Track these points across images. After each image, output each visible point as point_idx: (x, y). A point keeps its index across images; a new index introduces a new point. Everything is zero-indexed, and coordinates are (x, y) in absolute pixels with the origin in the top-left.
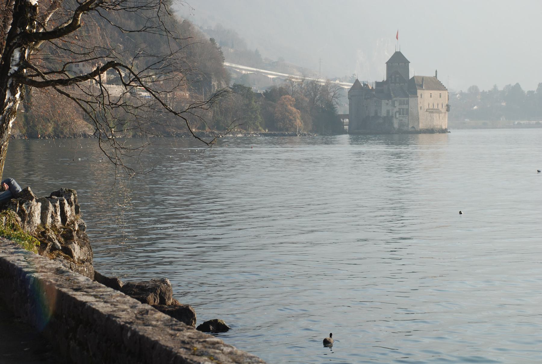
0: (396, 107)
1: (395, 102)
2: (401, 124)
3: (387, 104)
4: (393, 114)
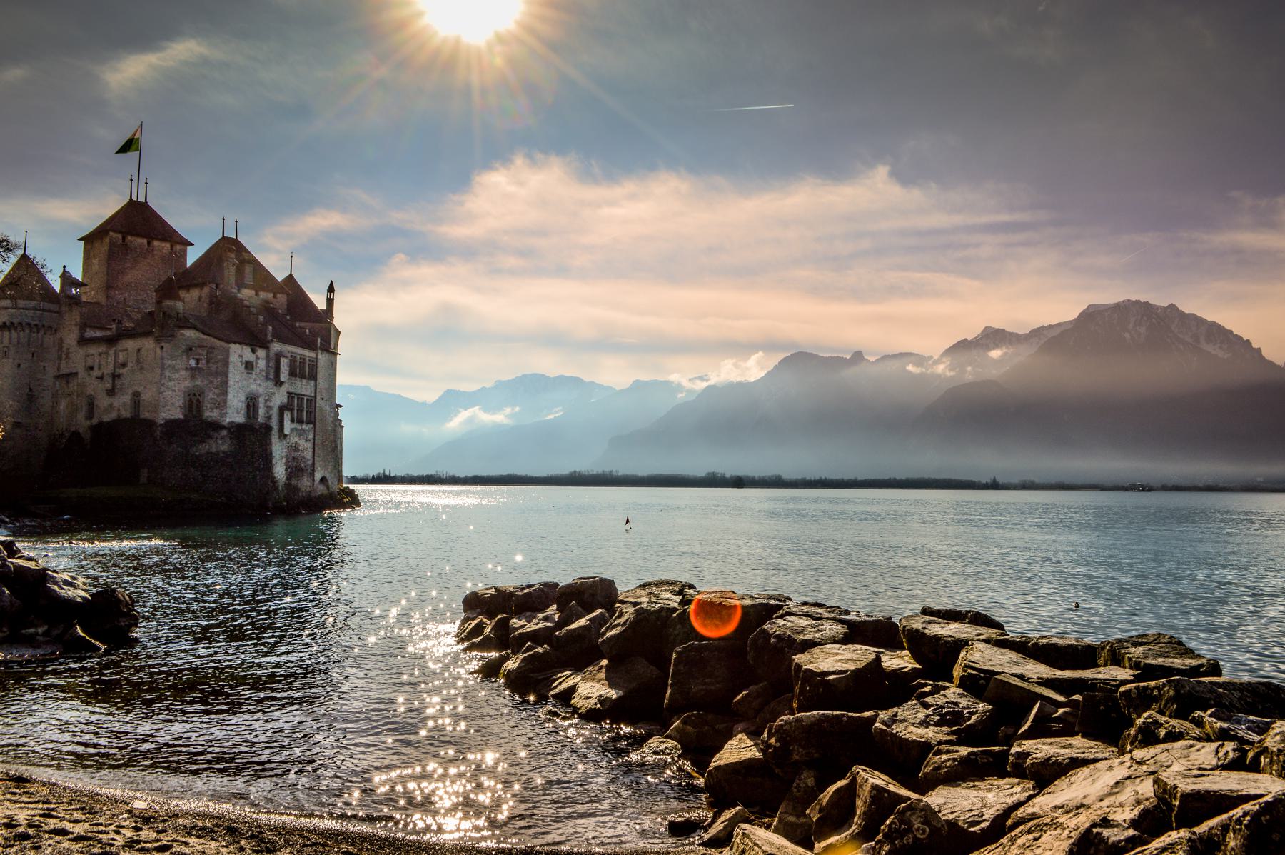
0: (282, 383)
1: (282, 359)
2: (296, 469)
3: (249, 366)
4: (269, 418)
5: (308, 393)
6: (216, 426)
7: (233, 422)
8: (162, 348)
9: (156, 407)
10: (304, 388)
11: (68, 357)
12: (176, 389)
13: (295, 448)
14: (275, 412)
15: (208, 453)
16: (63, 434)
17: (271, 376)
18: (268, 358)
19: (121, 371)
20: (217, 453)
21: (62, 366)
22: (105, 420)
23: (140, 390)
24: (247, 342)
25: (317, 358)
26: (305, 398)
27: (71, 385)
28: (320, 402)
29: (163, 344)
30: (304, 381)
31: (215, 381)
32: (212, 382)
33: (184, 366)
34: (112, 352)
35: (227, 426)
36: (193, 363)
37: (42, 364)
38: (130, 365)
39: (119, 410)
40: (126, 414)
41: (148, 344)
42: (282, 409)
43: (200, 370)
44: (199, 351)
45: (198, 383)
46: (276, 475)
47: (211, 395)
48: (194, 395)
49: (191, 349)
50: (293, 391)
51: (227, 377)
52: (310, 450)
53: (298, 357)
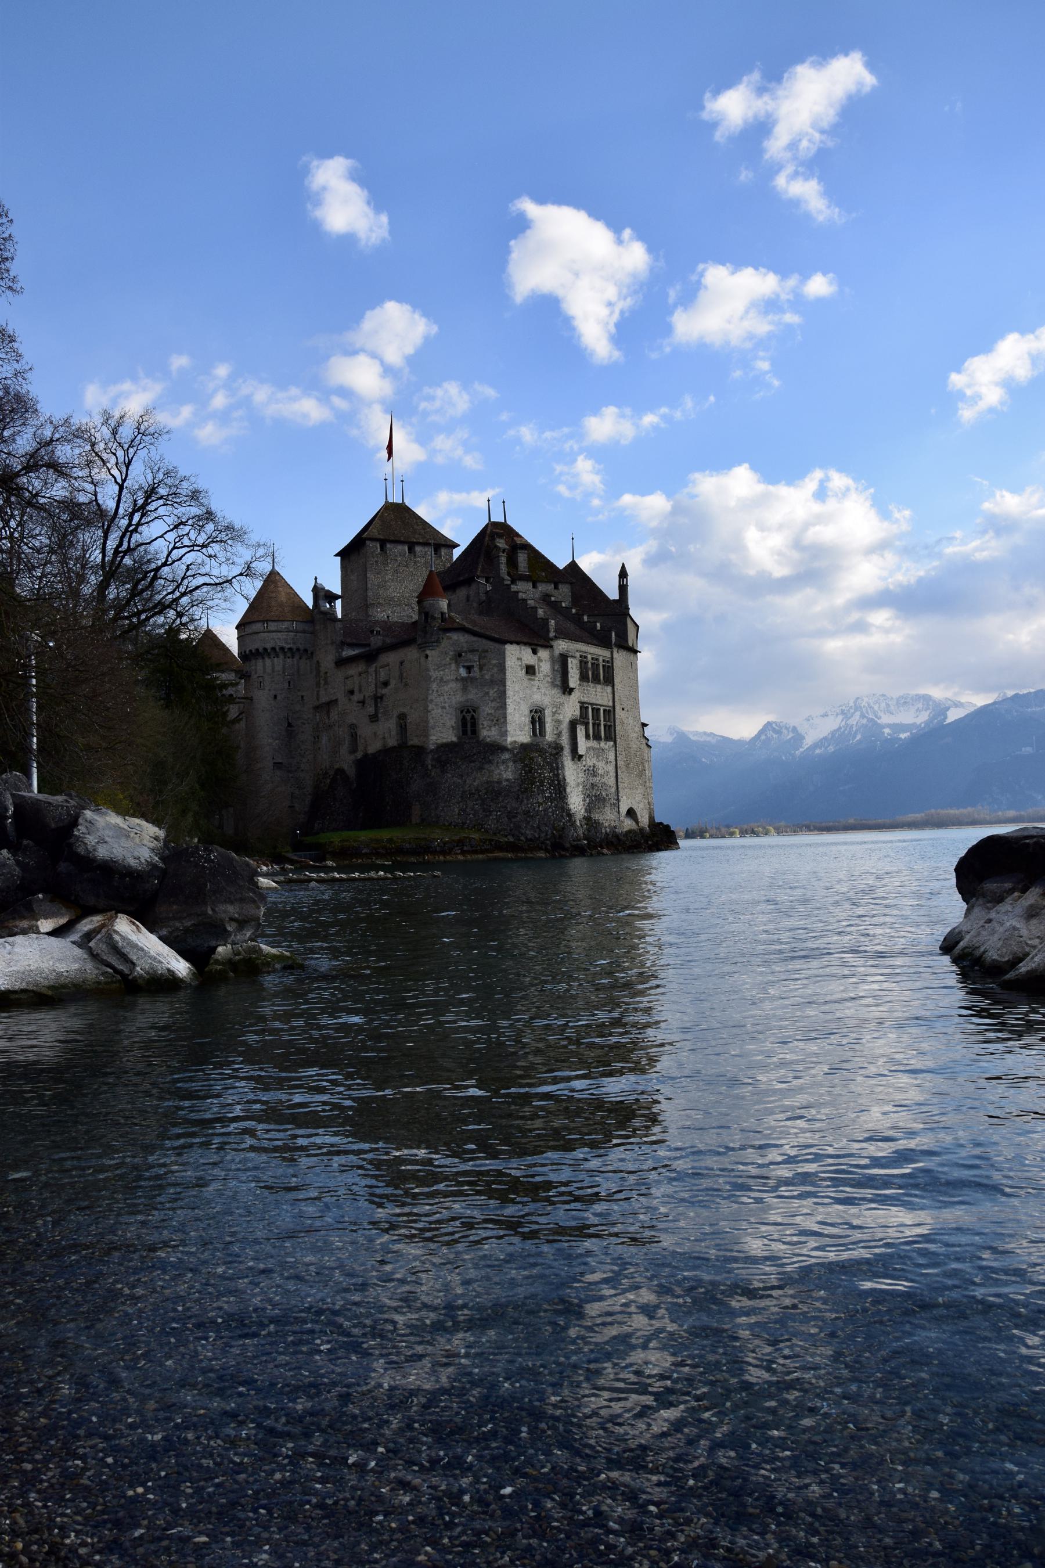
0: (571, 690)
1: (570, 660)
2: (595, 799)
3: (530, 670)
4: (559, 735)
5: (605, 703)
6: (497, 748)
7: (515, 742)
8: (427, 656)
9: (425, 733)
10: (599, 695)
11: (326, 683)
12: (447, 705)
13: (592, 772)
14: (565, 727)
15: (488, 782)
16: (326, 773)
17: (558, 683)
18: (552, 657)
19: (384, 691)
20: (499, 782)
21: (322, 692)
22: (370, 752)
23: (405, 711)
24: (525, 640)
25: (612, 658)
26: (602, 709)
27: (332, 715)
28: (619, 714)
29: (428, 652)
30: (599, 687)
31: (491, 692)
32: (487, 693)
33: (453, 677)
34: (372, 669)
35: (509, 747)
36: (463, 672)
37: (300, 694)
38: (393, 682)
39: (384, 738)
40: (392, 742)
41: (411, 654)
42: (573, 725)
43: (472, 680)
44: (470, 656)
45: (471, 696)
46: (572, 807)
47: (487, 709)
48: (468, 711)
49: (460, 655)
50: (585, 700)
51: (505, 686)
52: (612, 774)
53: (589, 657)
